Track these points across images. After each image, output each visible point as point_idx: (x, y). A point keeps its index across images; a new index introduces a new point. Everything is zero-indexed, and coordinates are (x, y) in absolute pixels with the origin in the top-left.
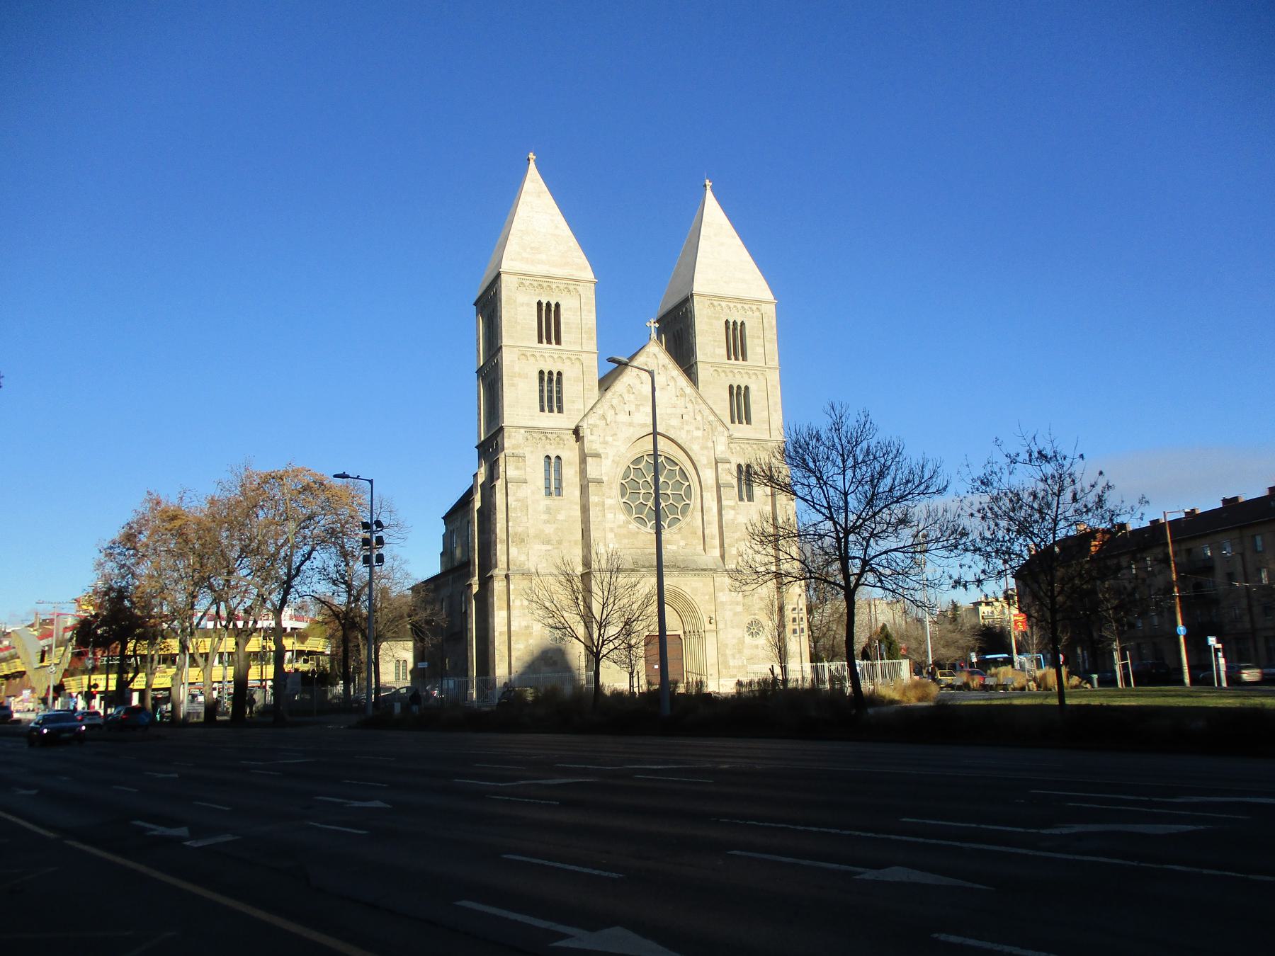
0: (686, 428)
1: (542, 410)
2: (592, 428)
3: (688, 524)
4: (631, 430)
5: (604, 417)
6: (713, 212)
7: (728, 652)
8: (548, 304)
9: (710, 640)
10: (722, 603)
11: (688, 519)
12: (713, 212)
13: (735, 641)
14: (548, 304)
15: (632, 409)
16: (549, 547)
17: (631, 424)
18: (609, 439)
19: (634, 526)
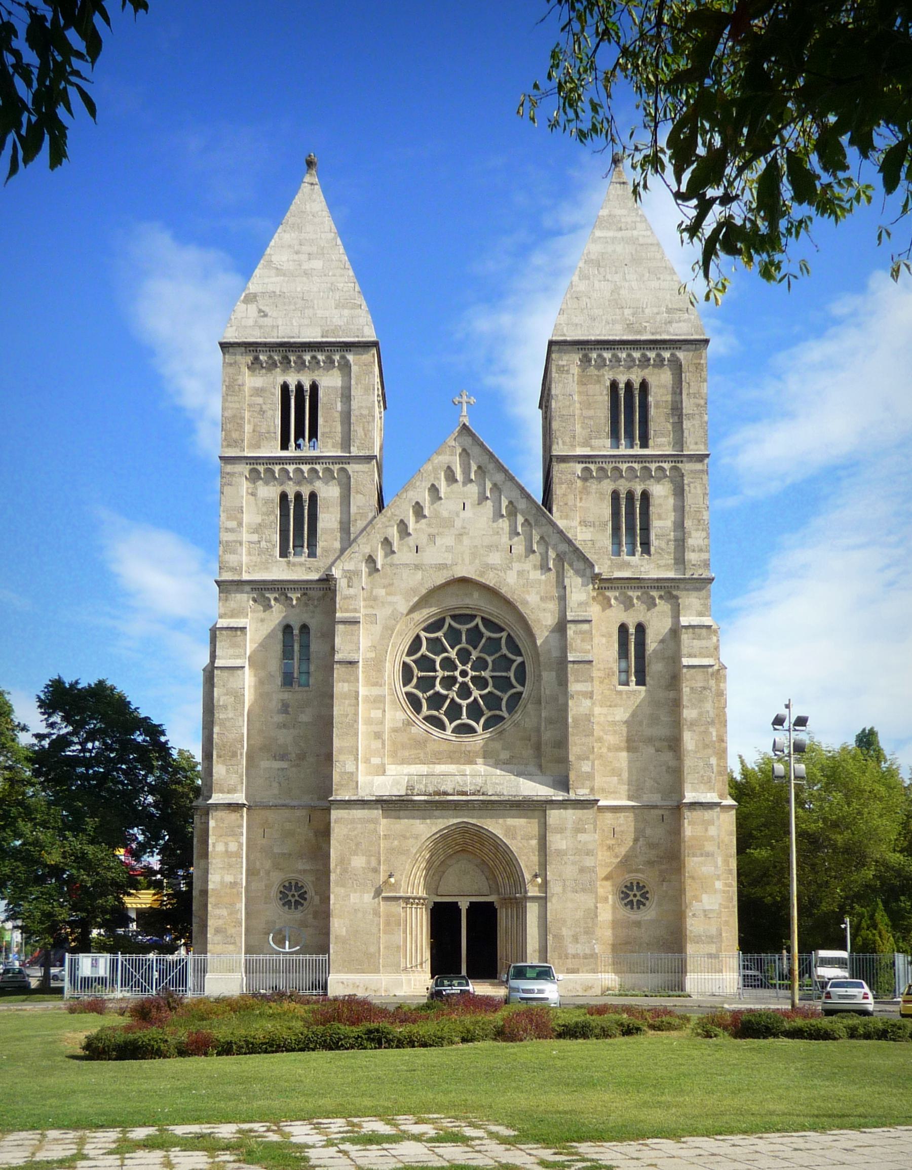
0: (516, 566)
1: (284, 553)
2: (350, 576)
3: (517, 725)
4: (419, 575)
5: (371, 560)
6: (849, 134)
7: (565, 931)
8: (300, 387)
9: (532, 911)
10: (559, 853)
11: (517, 716)
12: (849, 134)
13: (580, 914)
14: (300, 387)
15: (423, 540)
16: (284, 765)
17: (417, 567)
18: (381, 592)
19: (421, 728)
